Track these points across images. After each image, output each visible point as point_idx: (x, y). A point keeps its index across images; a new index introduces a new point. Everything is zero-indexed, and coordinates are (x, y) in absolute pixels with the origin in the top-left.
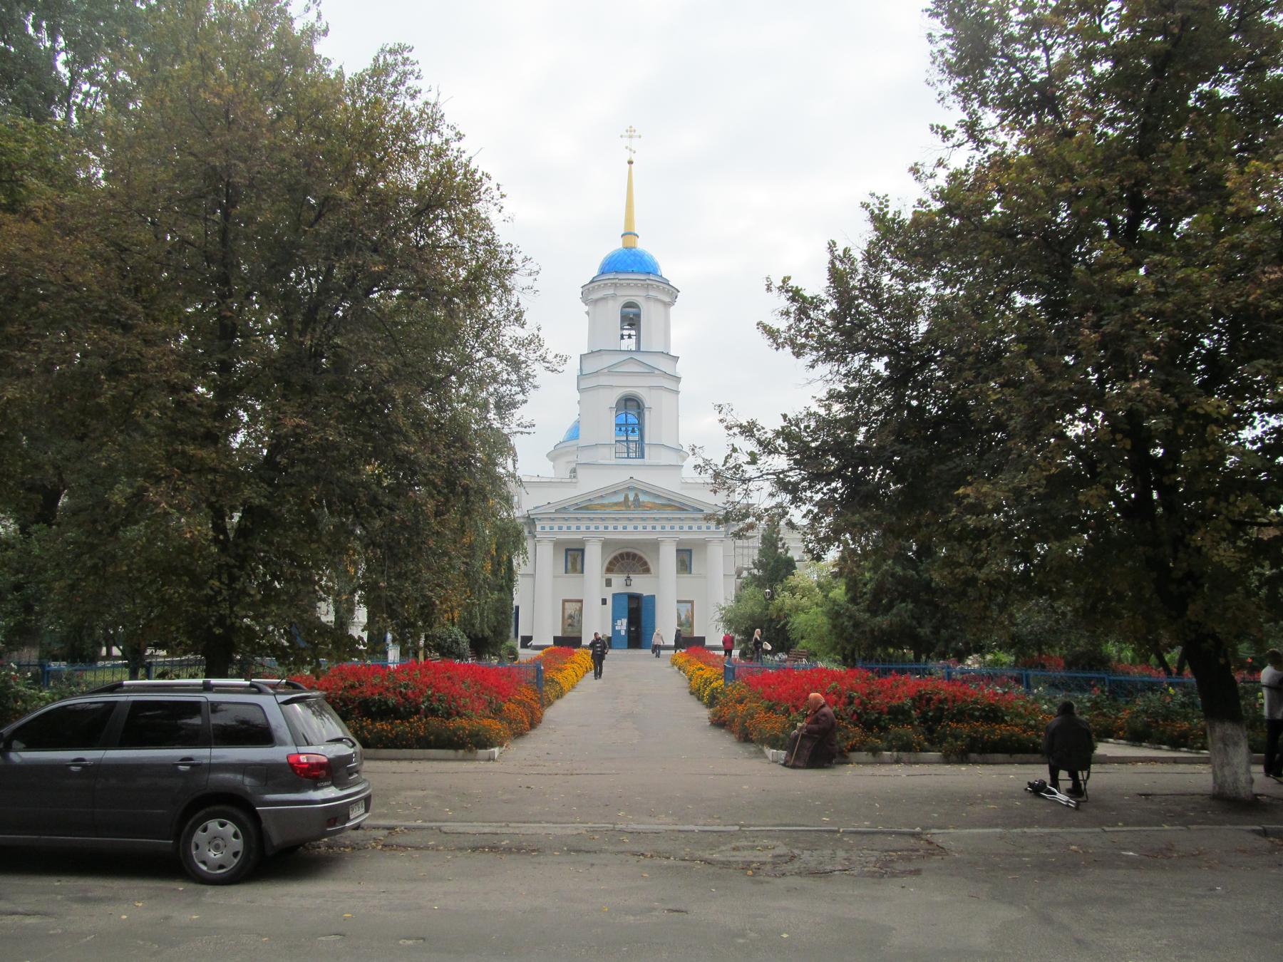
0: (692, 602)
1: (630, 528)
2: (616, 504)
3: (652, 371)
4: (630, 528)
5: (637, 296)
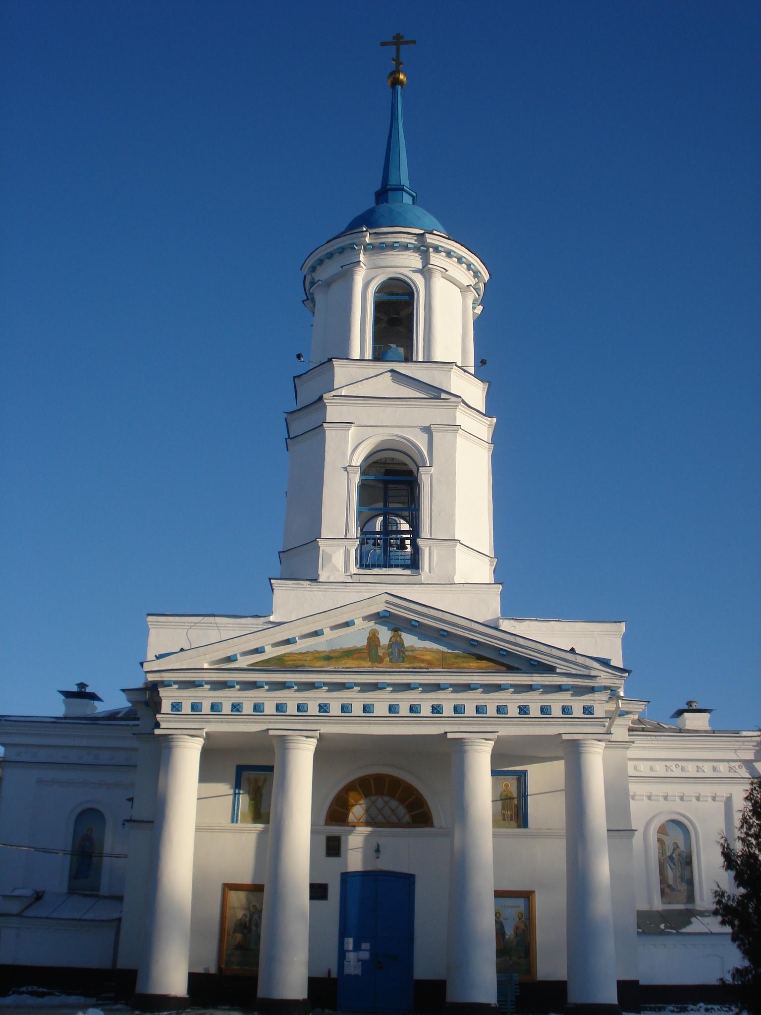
0: (527, 895)
1: (381, 709)
2: (349, 653)
3: (436, 393)
4: (381, 709)
5: (406, 264)
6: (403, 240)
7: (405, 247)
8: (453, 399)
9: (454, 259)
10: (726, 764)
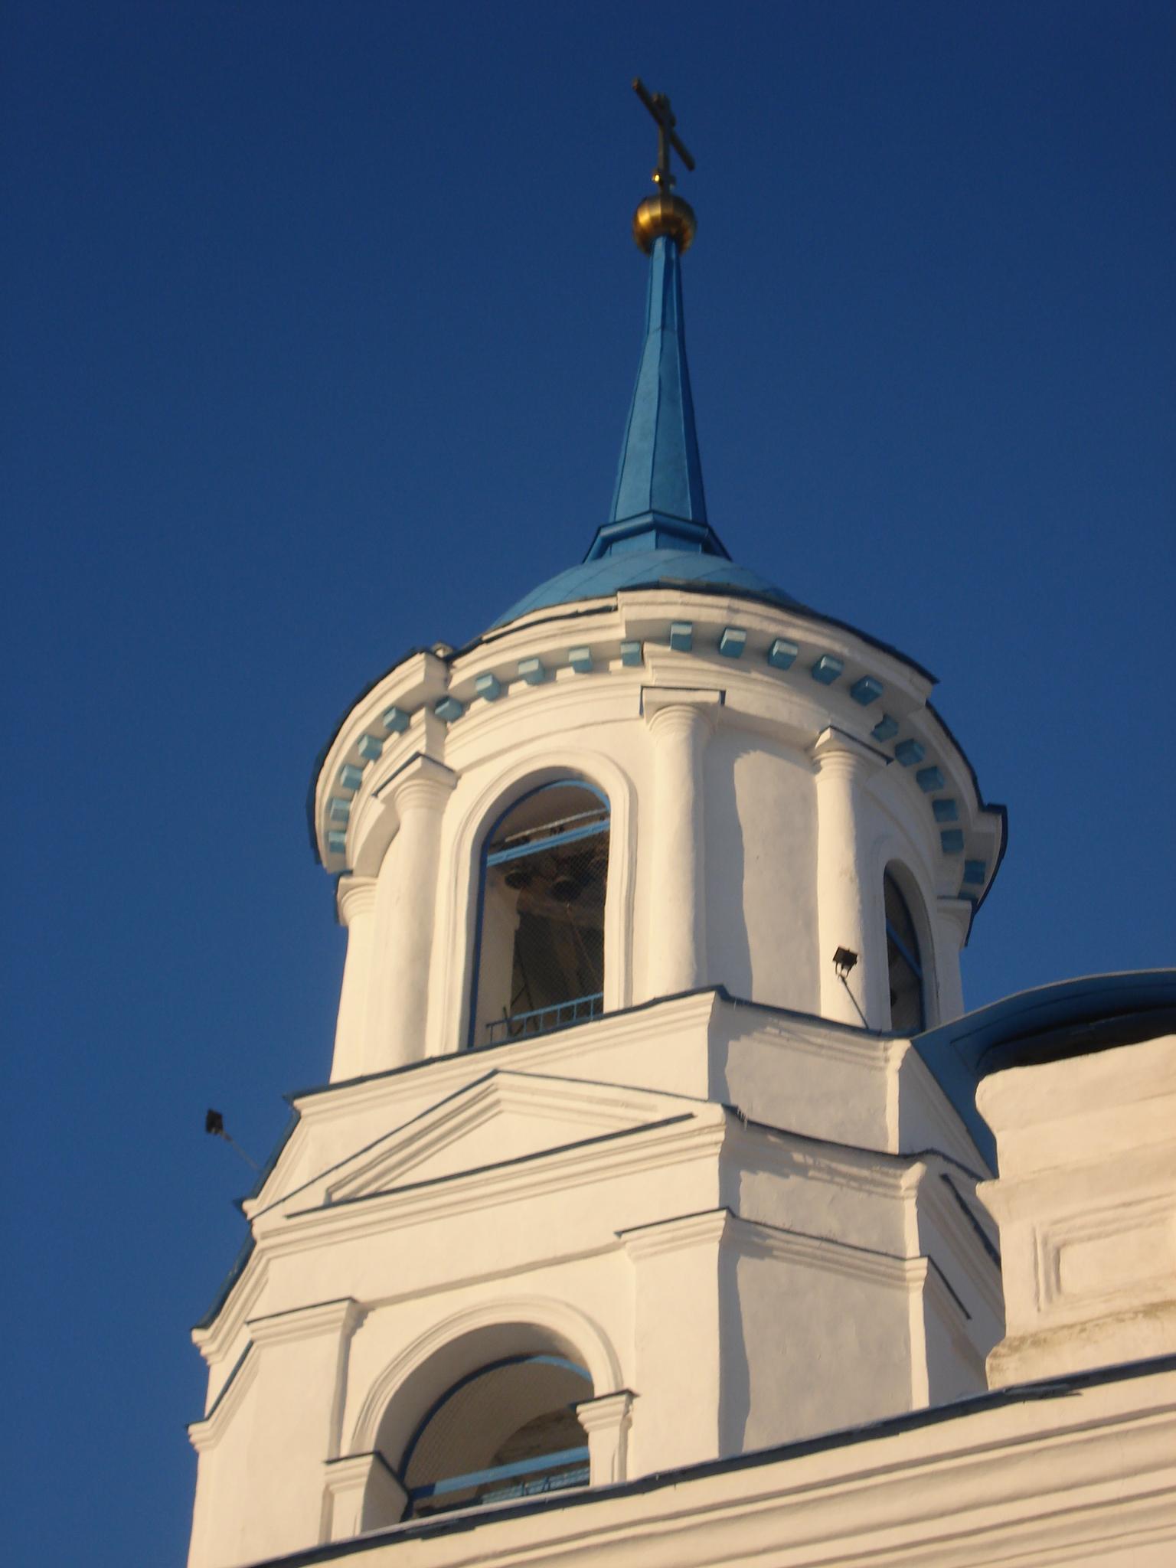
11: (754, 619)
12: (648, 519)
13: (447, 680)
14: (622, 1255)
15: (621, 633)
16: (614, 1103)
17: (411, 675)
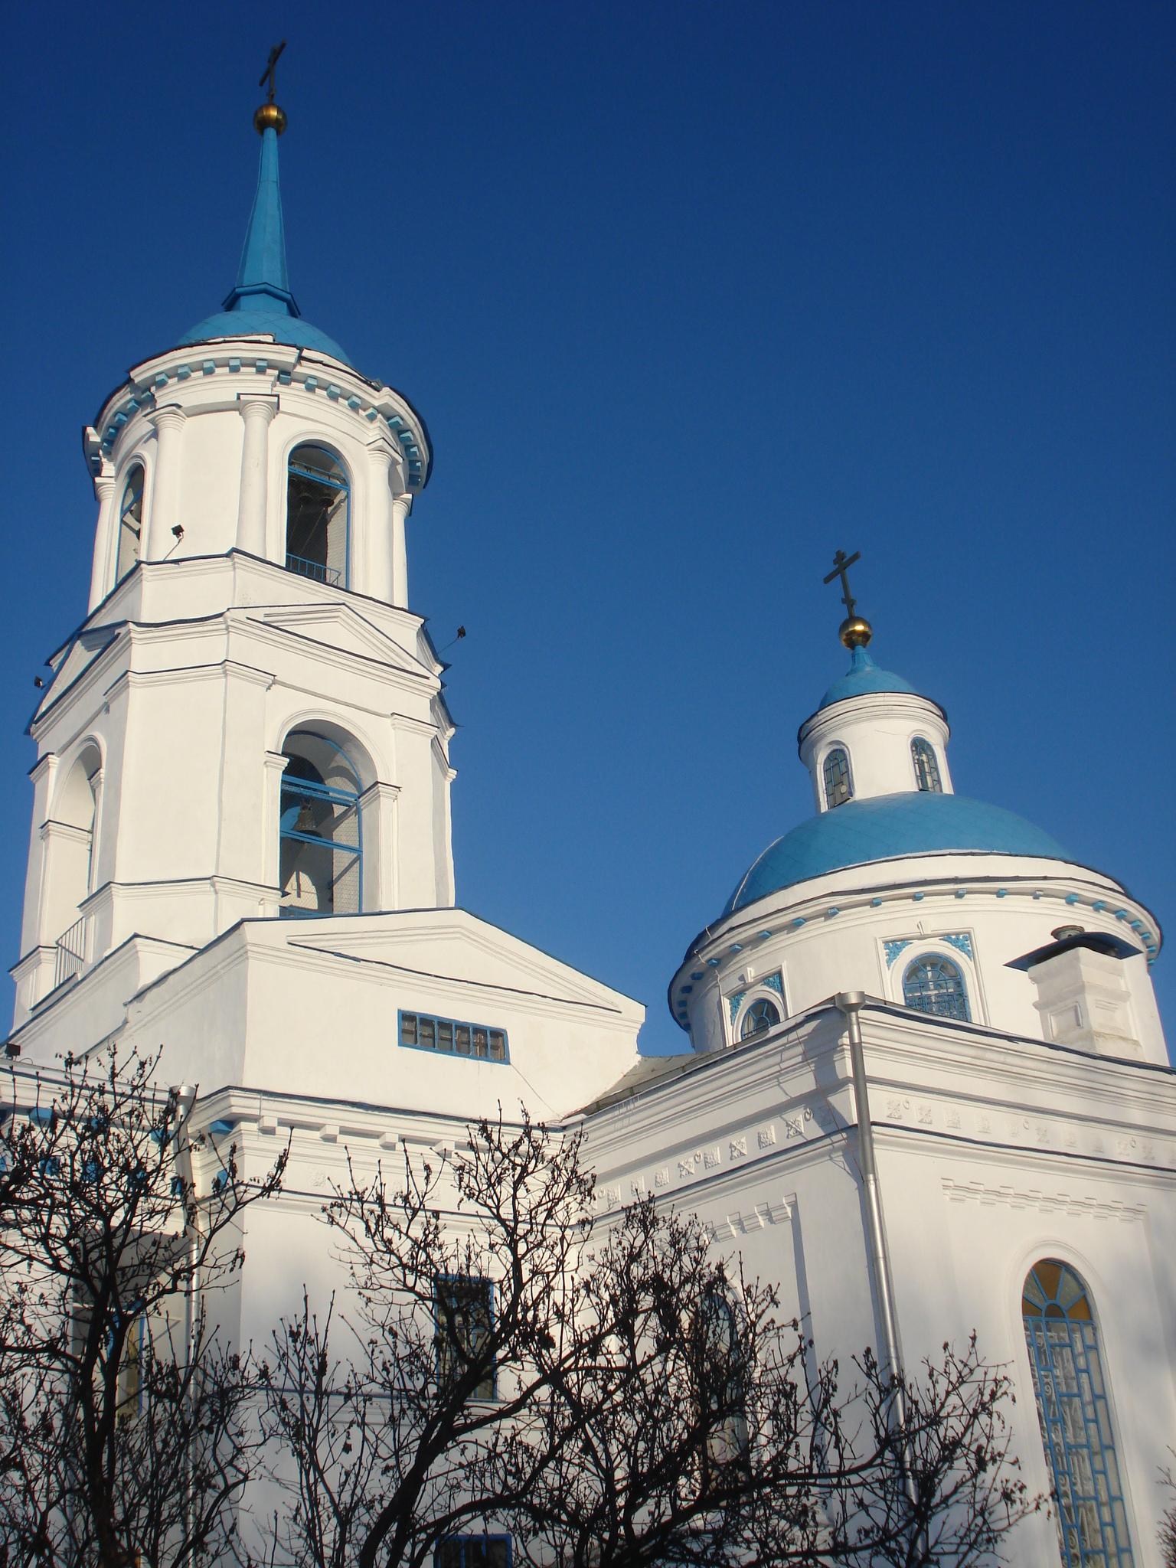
6: (119, 404)
7: (130, 414)
8: (122, 631)
9: (170, 381)
10: (777, 1120)
11: (417, 433)
12: (289, 296)
13: (295, 366)
14: (388, 721)
15: (376, 403)
16: (393, 651)
17: (288, 355)
